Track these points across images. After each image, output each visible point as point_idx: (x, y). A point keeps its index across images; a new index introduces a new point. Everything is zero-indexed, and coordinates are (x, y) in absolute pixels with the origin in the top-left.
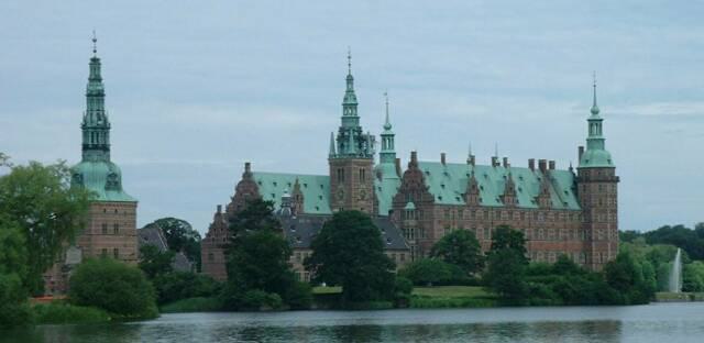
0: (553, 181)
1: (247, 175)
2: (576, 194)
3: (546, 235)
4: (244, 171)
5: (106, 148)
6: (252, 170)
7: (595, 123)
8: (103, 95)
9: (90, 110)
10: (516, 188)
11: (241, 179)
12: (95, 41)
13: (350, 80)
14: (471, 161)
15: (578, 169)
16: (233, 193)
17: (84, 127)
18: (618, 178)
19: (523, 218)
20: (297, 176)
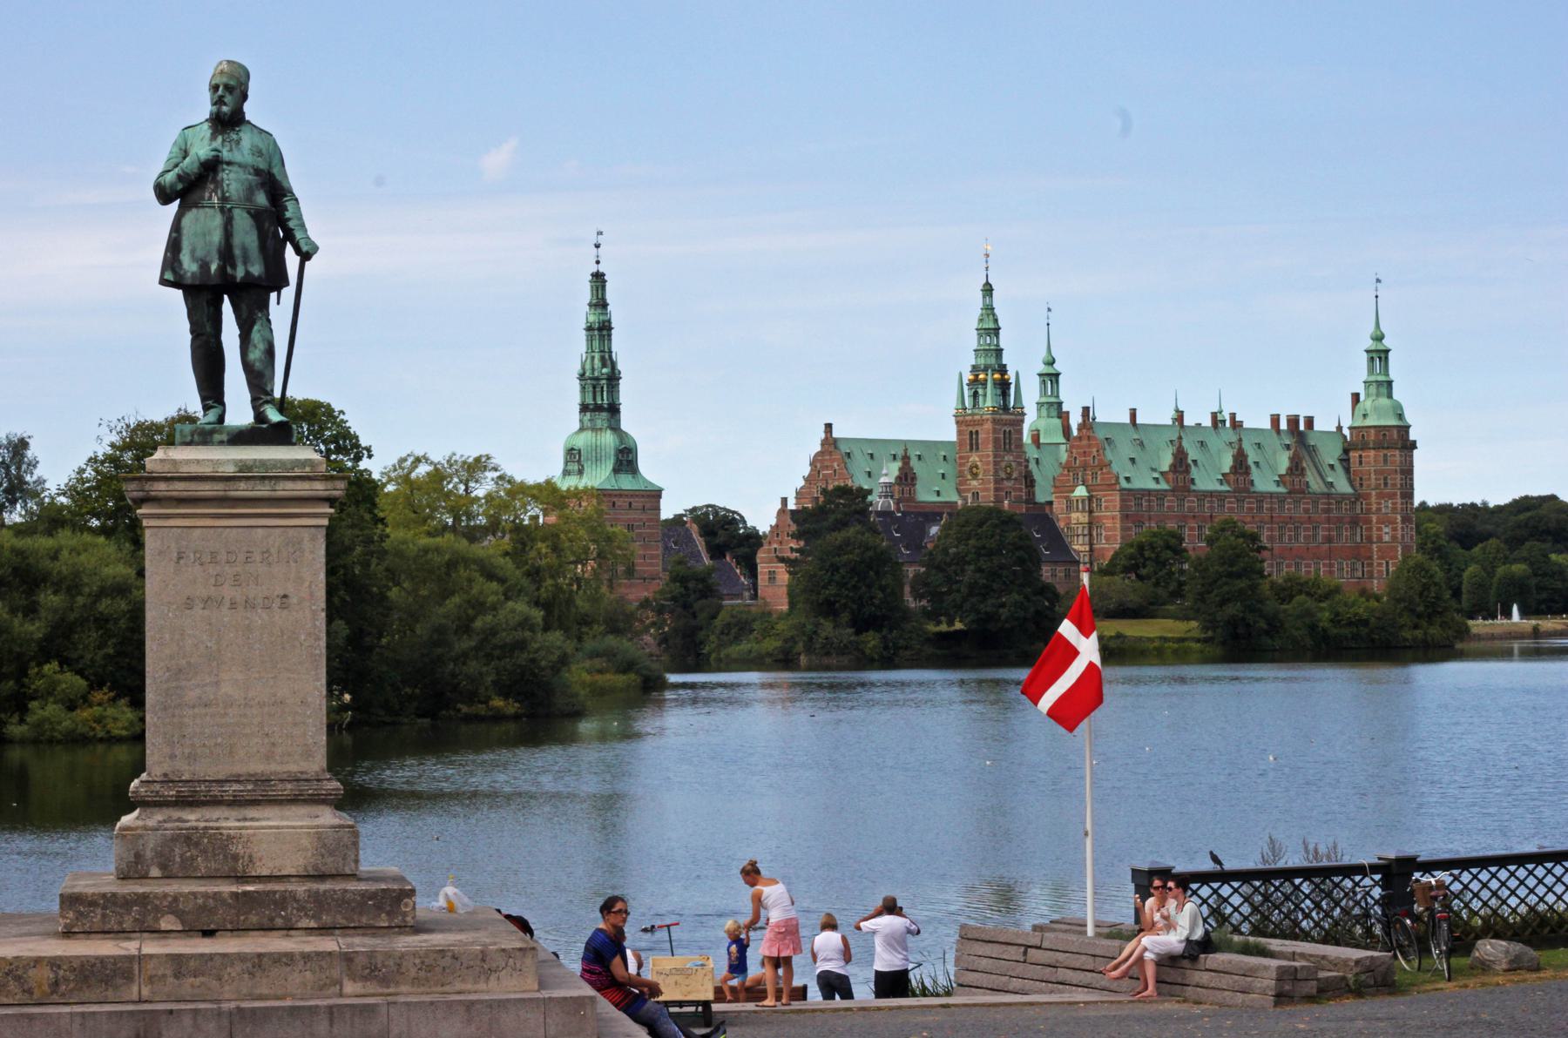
0: (1312, 451)
1: (830, 442)
2: (1347, 470)
3: (1297, 539)
4: (823, 436)
5: (614, 410)
6: (835, 435)
7: (1379, 356)
8: (610, 329)
9: (590, 349)
10: (1250, 461)
11: (818, 448)
12: (597, 246)
13: (988, 290)
14: (1180, 417)
15: (1350, 428)
16: (807, 471)
17: (582, 376)
18: (1415, 442)
19: (1260, 508)
20: (905, 442)
